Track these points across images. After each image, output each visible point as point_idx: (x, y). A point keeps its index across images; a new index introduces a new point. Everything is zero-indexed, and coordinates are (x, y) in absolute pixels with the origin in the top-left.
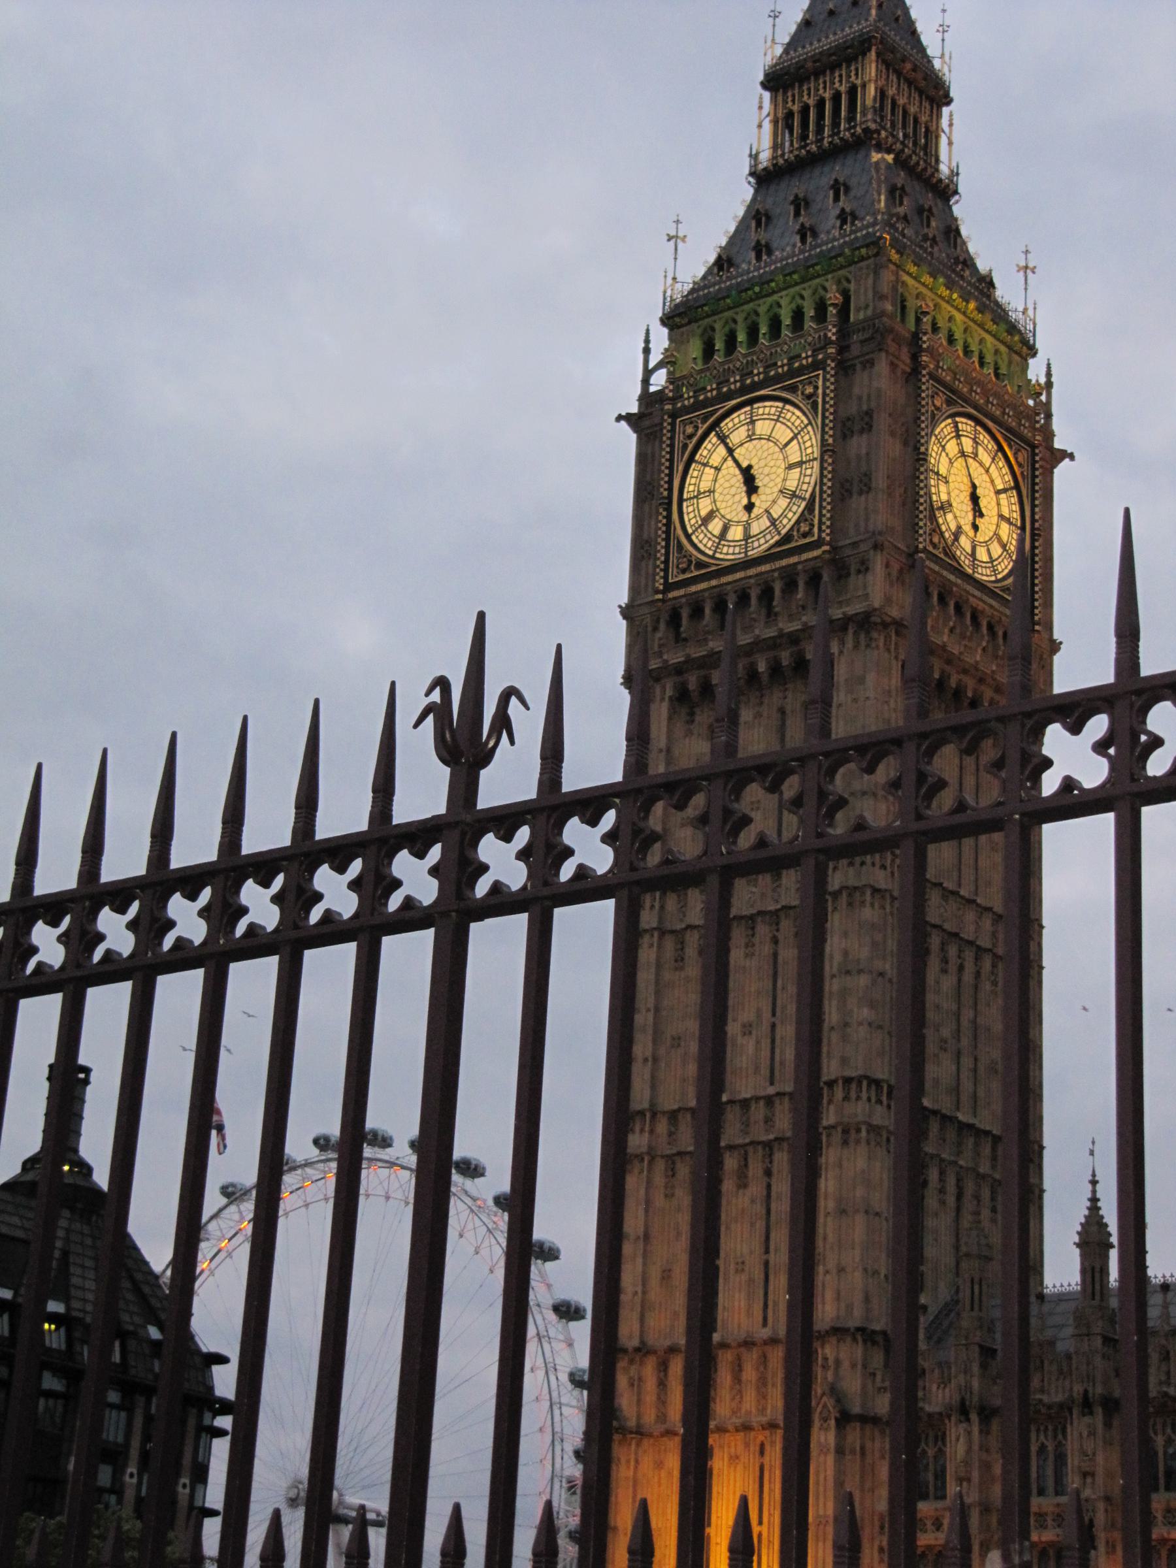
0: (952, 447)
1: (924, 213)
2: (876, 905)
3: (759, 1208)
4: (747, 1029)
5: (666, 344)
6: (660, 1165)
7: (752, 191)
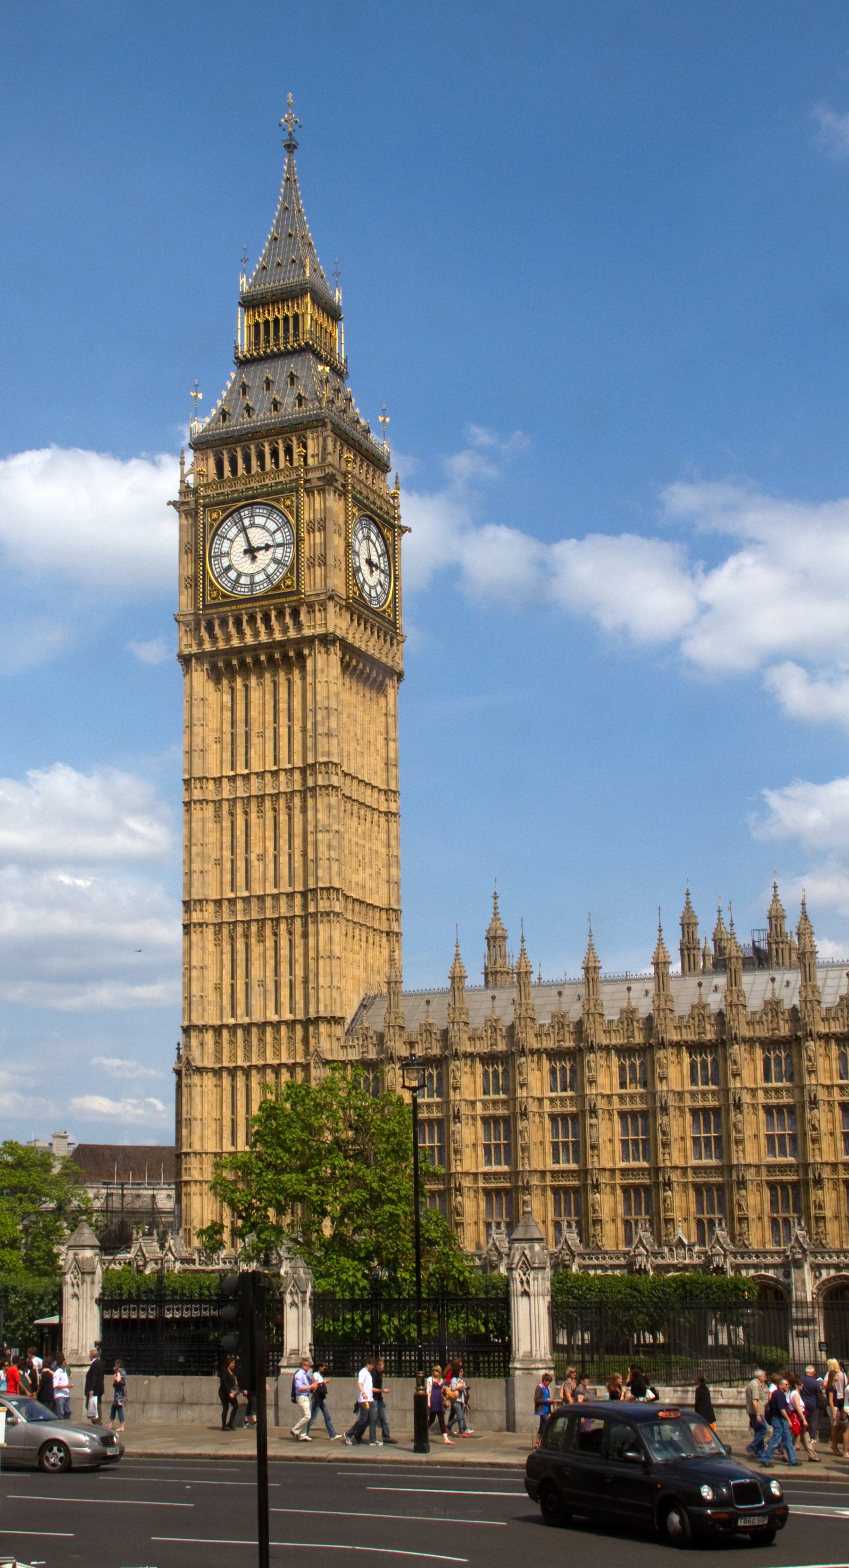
0: (360, 536)
3: (270, 953)
4: (262, 857)
6: (211, 929)
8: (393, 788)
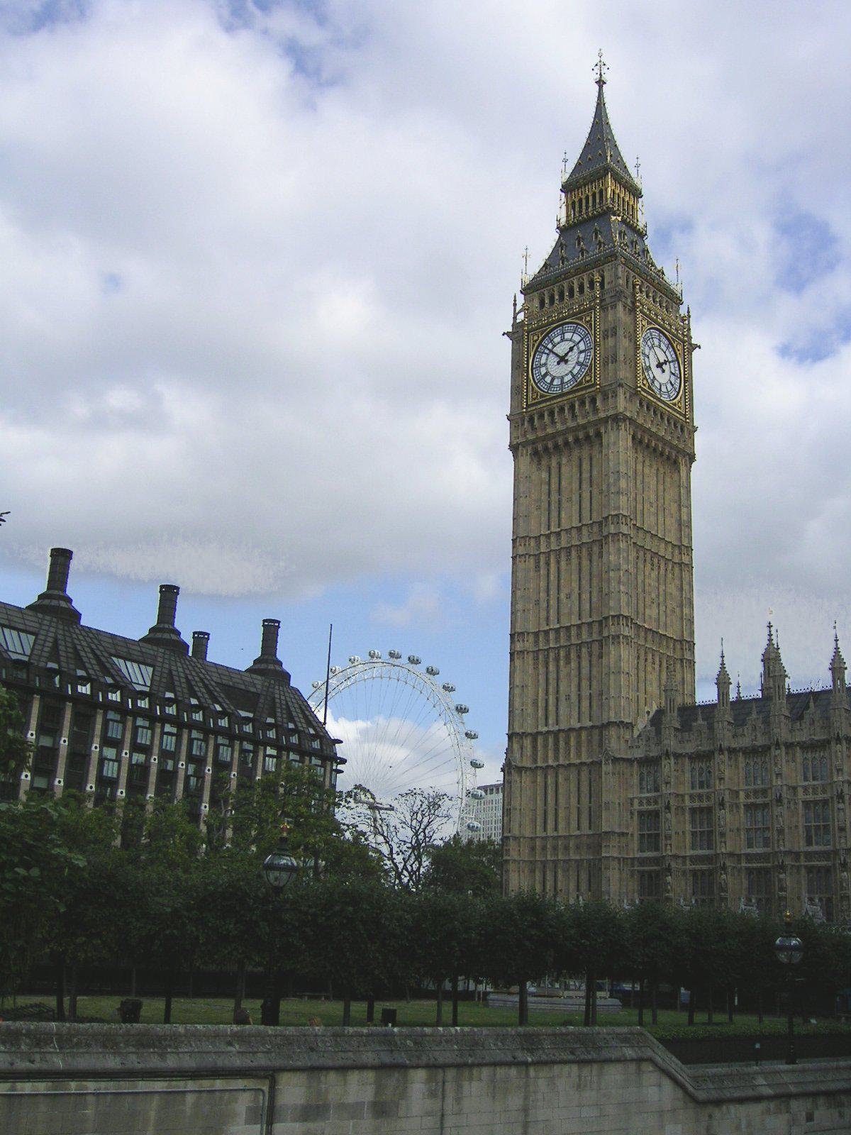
1: (633, 243)
3: (574, 673)
5: (523, 302)
6: (531, 656)
7: (558, 235)
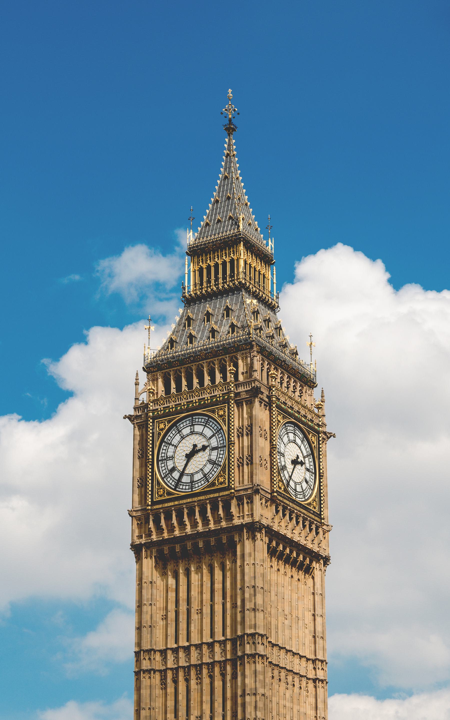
0: (285, 439)
1: (267, 321)
2: (260, 662)
5: (146, 380)
8: (320, 657)
